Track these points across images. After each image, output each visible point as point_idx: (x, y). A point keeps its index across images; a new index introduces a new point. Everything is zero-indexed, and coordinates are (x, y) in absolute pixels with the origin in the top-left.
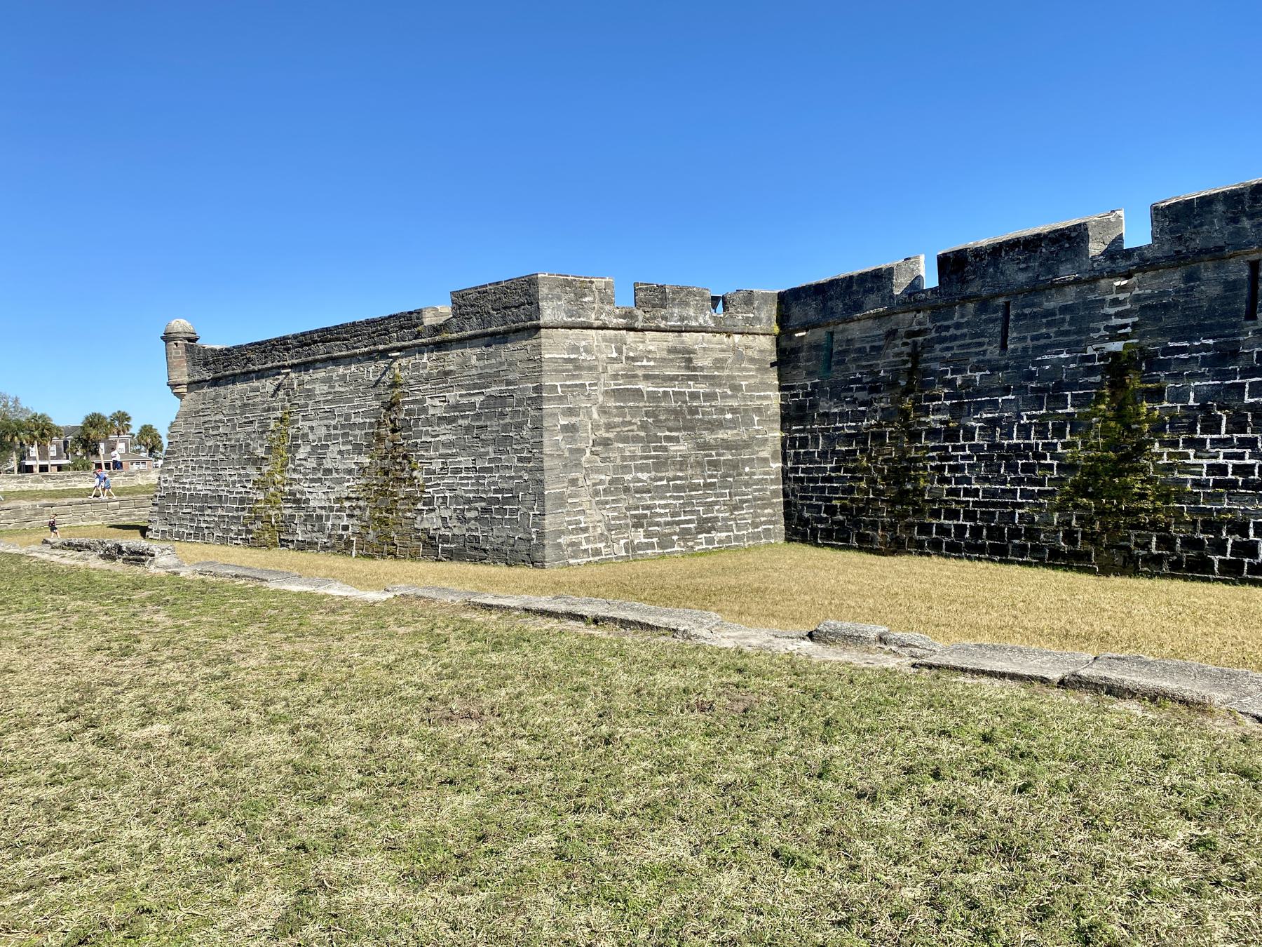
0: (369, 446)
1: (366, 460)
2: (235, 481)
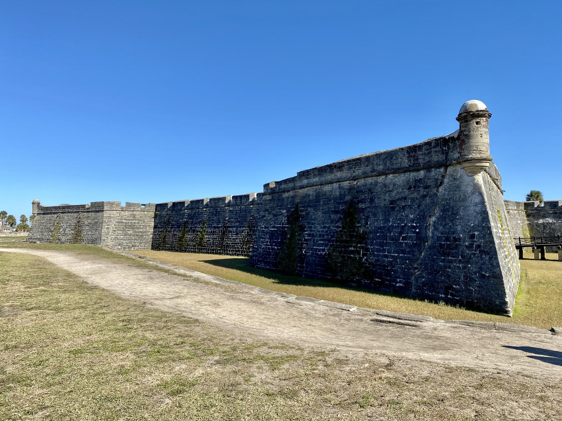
2: (46, 235)
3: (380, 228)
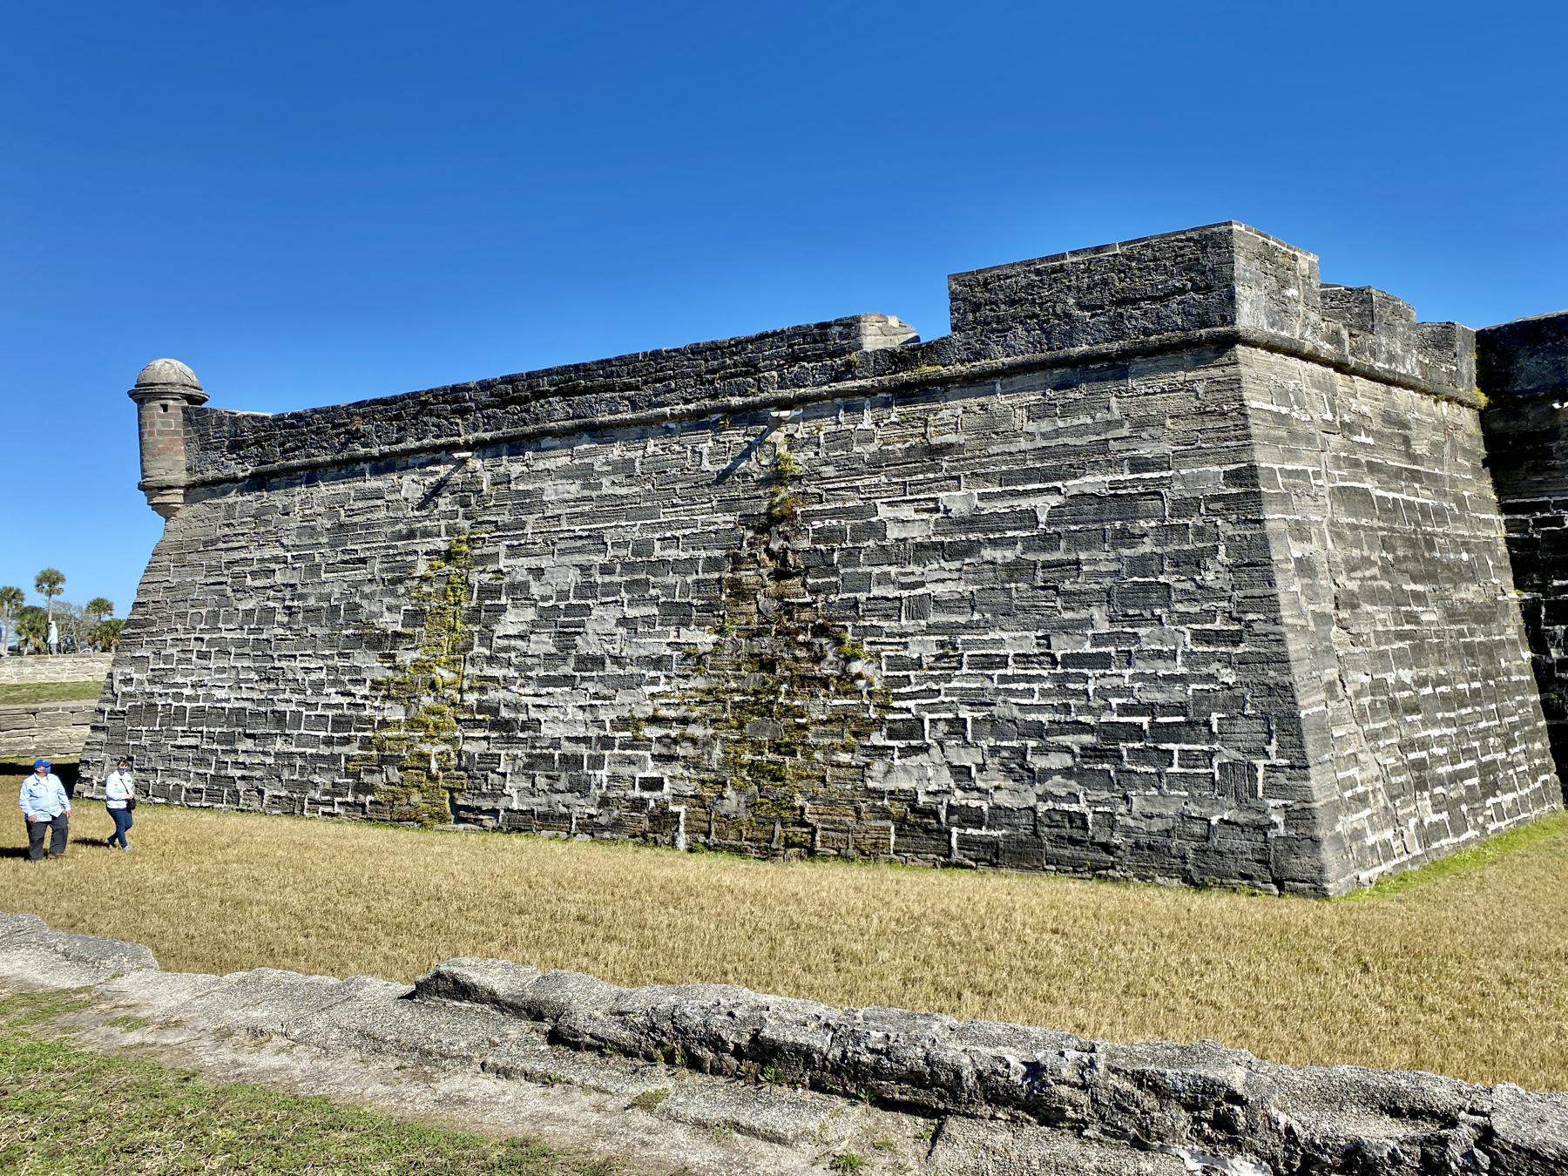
0: (710, 608)
1: (704, 639)
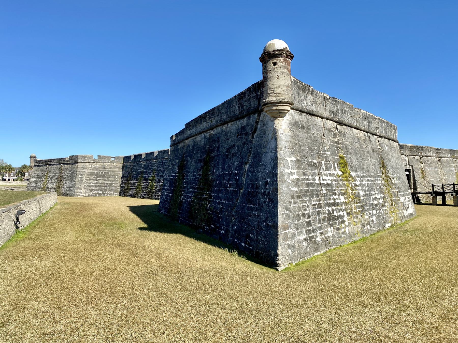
3: (220, 176)
